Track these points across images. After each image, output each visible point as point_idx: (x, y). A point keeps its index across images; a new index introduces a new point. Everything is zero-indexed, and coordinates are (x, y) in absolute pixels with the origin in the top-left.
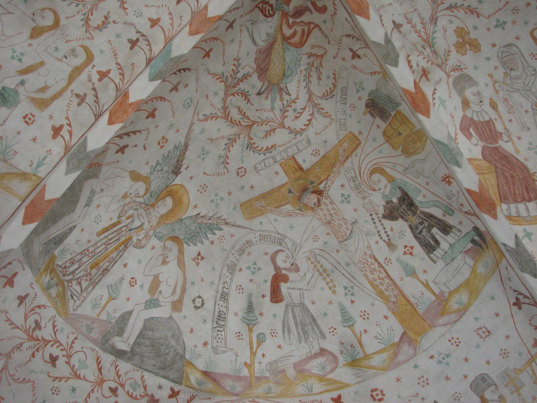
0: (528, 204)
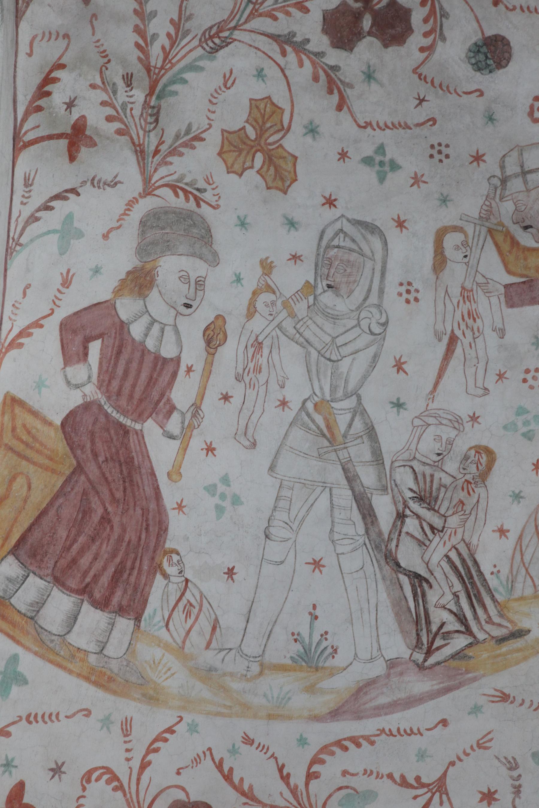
0: (86, 607)
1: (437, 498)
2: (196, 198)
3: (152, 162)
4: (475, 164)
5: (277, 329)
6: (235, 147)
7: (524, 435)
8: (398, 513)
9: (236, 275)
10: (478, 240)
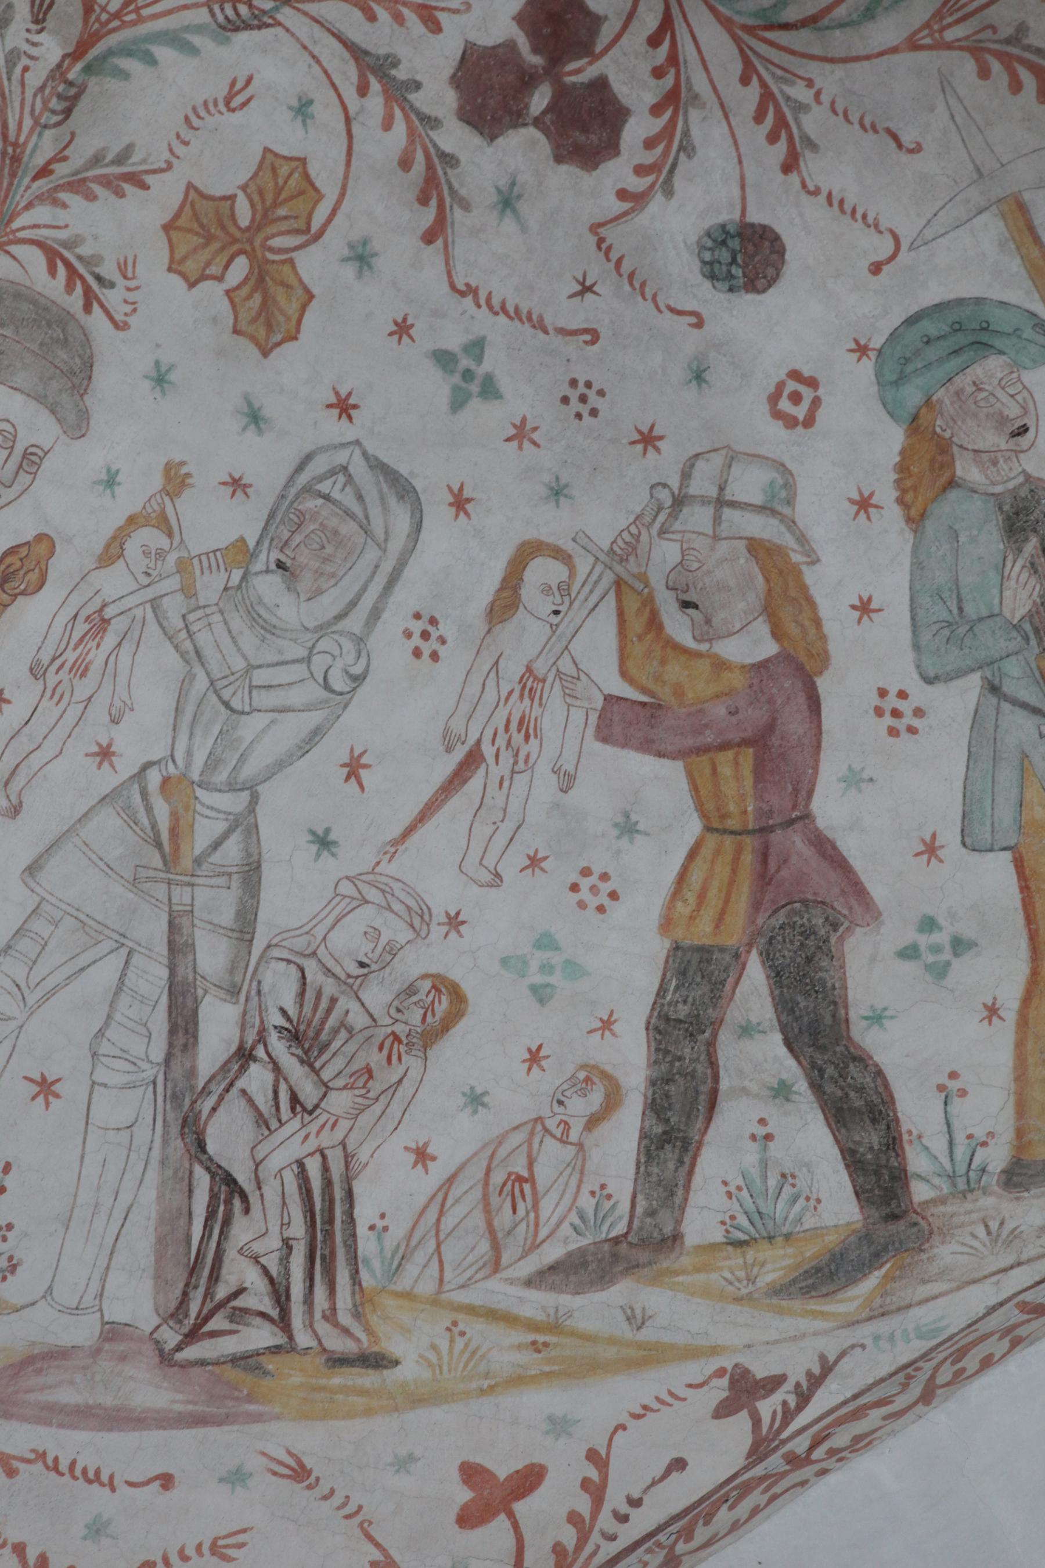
1: (326, 1046)
2: (88, 292)
3: (28, 188)
4: (640, 447)
5: (148, 606)
6: (202, 226)
7: (534, 989)
8: (241, 1048)
9: (109, 471)
10: (591, 591)
